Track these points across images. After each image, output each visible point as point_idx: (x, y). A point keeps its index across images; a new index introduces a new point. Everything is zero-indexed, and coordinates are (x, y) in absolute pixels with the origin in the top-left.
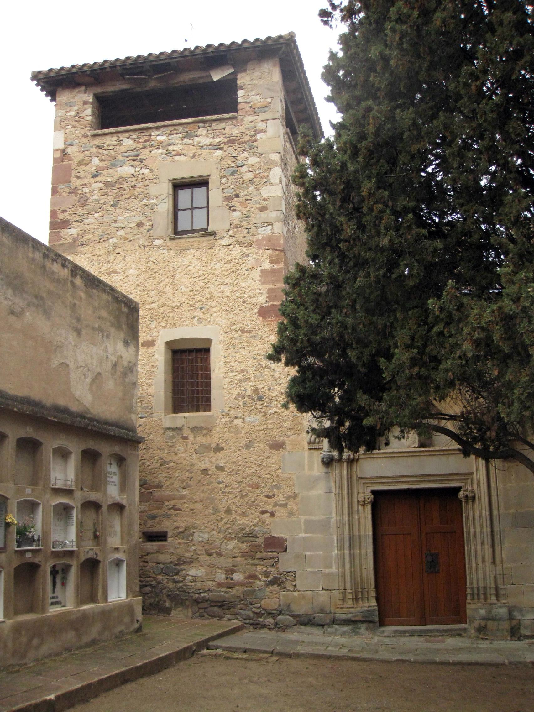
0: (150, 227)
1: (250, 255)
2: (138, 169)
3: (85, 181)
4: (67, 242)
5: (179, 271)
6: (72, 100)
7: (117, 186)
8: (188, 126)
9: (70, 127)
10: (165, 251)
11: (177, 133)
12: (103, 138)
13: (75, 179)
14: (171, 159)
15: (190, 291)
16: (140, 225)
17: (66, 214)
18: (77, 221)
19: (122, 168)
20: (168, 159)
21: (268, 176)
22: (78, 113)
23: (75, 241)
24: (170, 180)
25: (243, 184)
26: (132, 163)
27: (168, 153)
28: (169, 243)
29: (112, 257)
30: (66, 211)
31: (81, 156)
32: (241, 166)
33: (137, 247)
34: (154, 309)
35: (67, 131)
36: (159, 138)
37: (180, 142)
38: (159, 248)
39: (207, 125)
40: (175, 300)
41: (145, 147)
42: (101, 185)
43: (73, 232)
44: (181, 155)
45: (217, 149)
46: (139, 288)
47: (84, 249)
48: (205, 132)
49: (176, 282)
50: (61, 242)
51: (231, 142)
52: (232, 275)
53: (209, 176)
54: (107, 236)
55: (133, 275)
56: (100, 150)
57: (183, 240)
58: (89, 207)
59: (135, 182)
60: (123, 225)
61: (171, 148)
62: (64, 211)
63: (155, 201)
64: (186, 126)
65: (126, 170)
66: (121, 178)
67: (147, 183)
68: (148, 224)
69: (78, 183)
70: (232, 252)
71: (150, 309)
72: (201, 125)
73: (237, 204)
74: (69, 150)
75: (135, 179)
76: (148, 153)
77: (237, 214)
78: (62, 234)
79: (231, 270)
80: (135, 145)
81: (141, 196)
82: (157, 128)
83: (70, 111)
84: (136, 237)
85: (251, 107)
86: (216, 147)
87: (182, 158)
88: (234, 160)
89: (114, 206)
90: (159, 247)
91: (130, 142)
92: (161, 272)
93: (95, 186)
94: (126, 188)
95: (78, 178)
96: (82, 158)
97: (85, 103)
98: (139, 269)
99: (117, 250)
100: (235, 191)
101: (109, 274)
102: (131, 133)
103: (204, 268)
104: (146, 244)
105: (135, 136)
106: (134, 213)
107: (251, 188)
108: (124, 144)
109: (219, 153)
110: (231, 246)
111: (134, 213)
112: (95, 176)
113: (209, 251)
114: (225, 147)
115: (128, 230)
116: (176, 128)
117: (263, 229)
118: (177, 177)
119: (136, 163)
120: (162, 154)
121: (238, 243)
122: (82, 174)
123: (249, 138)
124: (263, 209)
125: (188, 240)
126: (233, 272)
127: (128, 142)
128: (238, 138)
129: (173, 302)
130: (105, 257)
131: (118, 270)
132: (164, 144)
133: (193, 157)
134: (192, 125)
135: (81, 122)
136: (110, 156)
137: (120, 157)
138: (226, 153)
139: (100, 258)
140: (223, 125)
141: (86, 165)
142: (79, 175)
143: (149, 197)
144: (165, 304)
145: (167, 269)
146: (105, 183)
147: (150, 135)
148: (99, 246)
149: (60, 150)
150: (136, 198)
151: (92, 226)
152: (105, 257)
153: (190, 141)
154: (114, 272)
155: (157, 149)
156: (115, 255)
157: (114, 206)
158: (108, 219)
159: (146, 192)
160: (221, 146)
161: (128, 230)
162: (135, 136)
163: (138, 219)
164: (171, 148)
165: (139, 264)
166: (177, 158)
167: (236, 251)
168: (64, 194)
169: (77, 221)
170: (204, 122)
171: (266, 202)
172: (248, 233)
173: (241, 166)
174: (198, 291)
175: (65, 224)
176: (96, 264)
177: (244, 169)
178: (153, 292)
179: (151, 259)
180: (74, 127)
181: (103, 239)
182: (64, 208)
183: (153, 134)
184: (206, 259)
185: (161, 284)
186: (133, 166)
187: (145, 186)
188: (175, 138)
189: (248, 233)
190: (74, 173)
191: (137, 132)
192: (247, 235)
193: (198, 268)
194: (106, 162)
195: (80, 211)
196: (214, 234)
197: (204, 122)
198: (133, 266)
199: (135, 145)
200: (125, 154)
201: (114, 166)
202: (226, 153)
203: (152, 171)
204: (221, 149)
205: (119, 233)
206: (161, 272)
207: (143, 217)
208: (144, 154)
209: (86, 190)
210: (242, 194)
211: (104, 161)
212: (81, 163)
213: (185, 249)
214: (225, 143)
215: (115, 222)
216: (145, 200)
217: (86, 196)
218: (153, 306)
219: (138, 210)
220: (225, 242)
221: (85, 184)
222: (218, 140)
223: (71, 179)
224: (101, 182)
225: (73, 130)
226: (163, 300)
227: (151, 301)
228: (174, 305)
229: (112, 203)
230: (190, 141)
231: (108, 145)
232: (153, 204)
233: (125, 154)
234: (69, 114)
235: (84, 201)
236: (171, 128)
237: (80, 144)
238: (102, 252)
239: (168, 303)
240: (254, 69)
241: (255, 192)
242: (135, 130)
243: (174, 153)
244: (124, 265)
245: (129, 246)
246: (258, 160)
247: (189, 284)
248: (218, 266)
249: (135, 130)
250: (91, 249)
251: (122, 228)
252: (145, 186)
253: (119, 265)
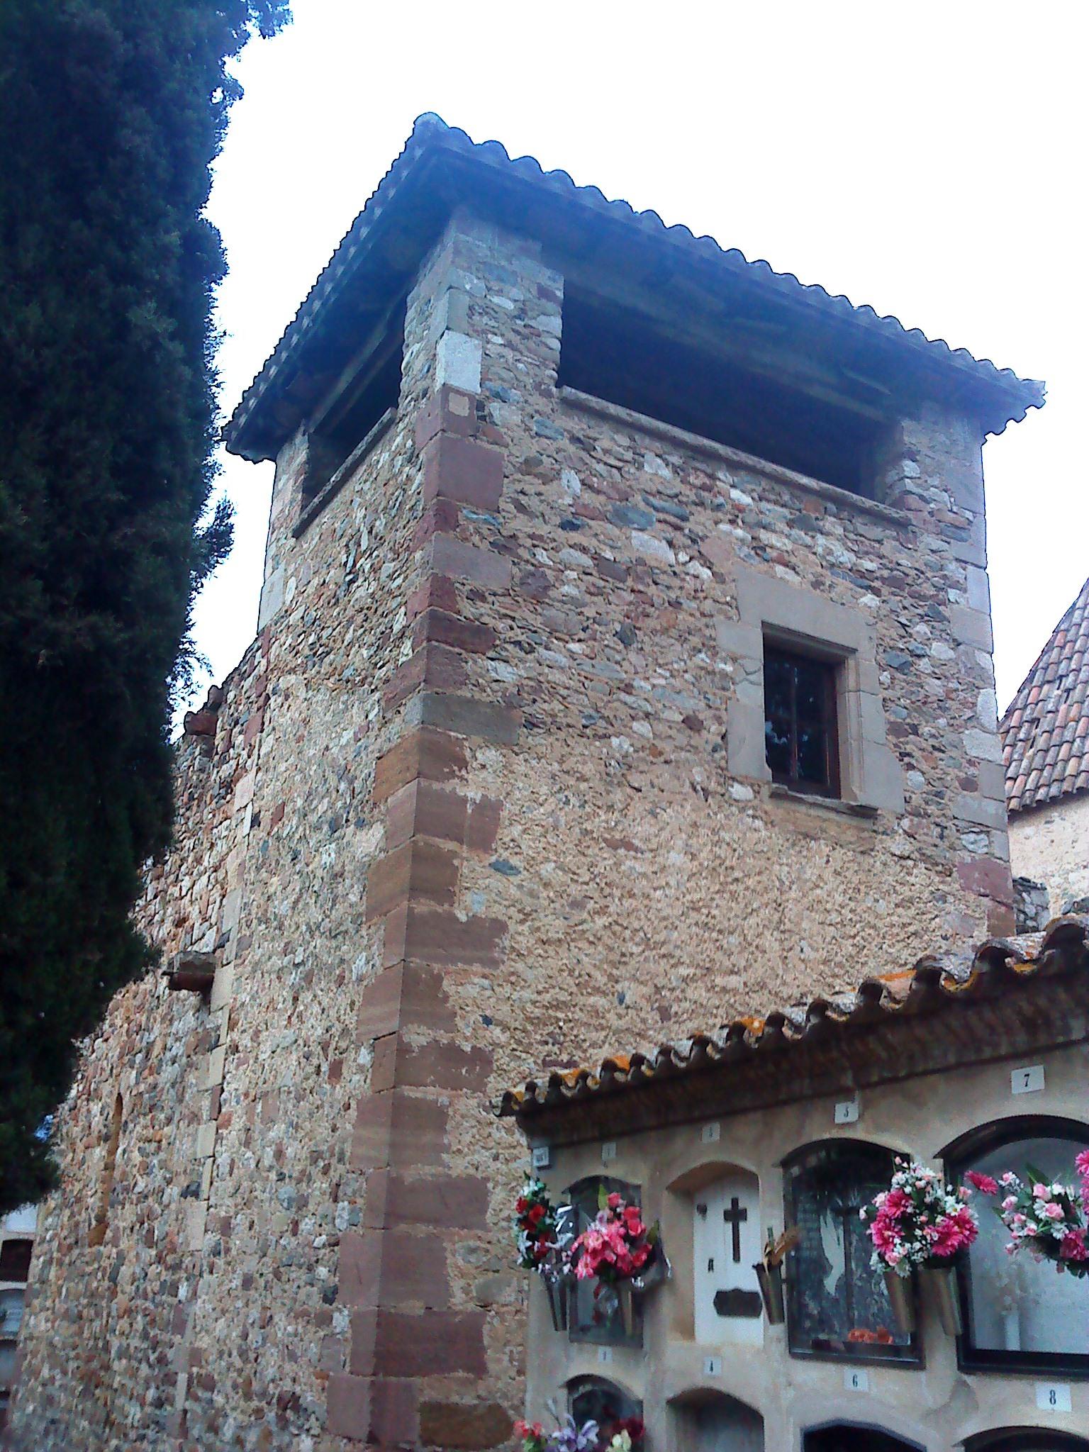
0: (720, 741)
1: (950, 899)
2: (683, 557)
3: (543, 530)
4: (484, 697)
5: (793, 894)
6: (503, 263)
7: (630, 582)
8: (806, 498)
9: (500, 340)
10: (758, 823)
11: (776, 503)
12: (592, 423)
13: (511, 507)
14: (764, 566)
15: (826, 962)
16: (692, 723)
17: (484, 608)
18: (518, 643)
19: (645, 536)
20: (758, 565)
21: (974, 704)
22: (523, 311)
23: (511, 703)
24: (764, 624)
25: (925, 703)
26: (671, 534)
27: (760, 549)
28: (769, 806)
29: (618, 796)
30: (483, 599)
31: (531, 448)
32: (919, 656)
33: (687, 788)
34: (735, 991)
35: (492, 349)
36: (735, 494)
37: (786, 530)
38: (742, 810)
39: (845, 515)
40: (788, 978)
41: (701, 504)
42: (586, 561)
43: (505, 672)
44: (786, 565)
45: (869, 588)
46: (693, 914)
47: (538, 740)
48: (840, 531)
49: (788, 926)
50: (465, 693)
51: (897, 583)
52: (915, 942)
53: (854, 651)
54: (602, 723)
55: (680, 871)
56: (584, 454)
57: (803, 809)
58: (553, 612)
59: (679, 593)
60: (650, 709)
61: (765, 536)
62: (476, 596)
63: (729, 668)
64: (798, 493)
65: (650, 545)
66: (641, 561)
67: (708, 606)
68: (713, 728)
69: (519, 524)
70: (912, 879)
71: (724, 990)
72: (832, 507)
73: (917, 754)
74: (495, 408)
75: (677, 582)
76: (709, 524)
77: (916, 777)
78: (469, 667)
79: (911, 929)
80: (678, 487)
81: (695, 640)
82: (734, 466)
83: (500, 293)
84: (683, 754)
85: (931, 513)
86: (864, 580)
87: (790, 576)
88: (902, 632)
89: (625, 638)
90: (743, 806)
91: (666, 473)
92: (750, 882)
93: (568, 554)
94: (657, 601)
95: (521, 508)
96: (533, 453)
97: (544, 293)
98: (694, 857)
99: (636, 779)
100: (909, 715)
101: (613, 845)
102: (668, 448)
103: (852, 904)
104: (713, 786)
105: (675, 459)
106: (677, 683)
107: (942, 722)
108: (646, 468)
109: (869, 599)
110: (910, 863)
111: (677, 683)
112: (568, 526)
113: (860, 858)
114: (885, 590)
115: (661, 728)
116: (777, 488)
117: (972, 837)
118: (782, 624)
119: (679, 539)
120: (742, 540)
121: (925, 858)
122: (532, 503)
123: (932, 592)
124: (969, 785)
125: (813, 812)
126: (915, 934)
127: (657, 470)
128: (909, 580)
129: (784, 983)
130: (601, 789)
131: (636, 842)
132: (751, 518)
133: (817, 584)
134: (814, 498)
135: (531, 344)
136: (613, 485)
137: (638, 498)
138: (887, 607)
139: (583, 786)
140: (877, 532)
141: (546, 480)
142: (524, 500)
143: (714, 652)
144: (763, 986)
145: (764, 878)
146: (597, 557)
147: (712, 477)
148: (579, 747)
149: (471, 397)
150: (682, 639)
151: (556, 676)
152: (601, 789)
153: (808, 540)
154: (629, 846)
155: (732, 522)
156: (629, 790)
157: (625, 638)
158: (604, 671)
159: (707, 632)
160: (877, 584)
161: (661, 728)
162: (675, 459)
163: (693, 704)
164: (765, 536)
165: (693, 841)
166: (780, 569)
167: (920, 875)
168: (476, 539)
169: (518, 643)
170: (841, 503)
171: (972, 771)
172: (942, 837)
173: (919, 656)
174: (840, 965)
175: (479, 638)
176: (573, 800)
177: (924, 664)
178: (732, 939)
179: (726, 836)
180: (509, 345)
181: (596, 727)
182: (477, 584)
183: (720, 475)
184: (855, 880)
185: (752, 921)
186: (670, 544)
187: (703, 615)
188: (775, 513)
189: (942, 837)
190: (509, 488)
191: (682, 452)
192: (938, 841)
193: (839, 899)
194: (602, 498)
195: (524, 613)
196: (865, 813)
197: (841, 503)
198: (680, 843)
199: (678, 487)
200: (656, 501)
201: (621, 518)
202: (887, 607)
203: (719, 577)
204: (876, 592)
205: (635, 725)
206: (750, 882)
207: (702, 704)
208: (700, 521)
209: (542, 556)
210: (925, 729)
211: (598, 492)
212: (529, 466)
213: (806, 836)
214: (883, 579)
215: (628, 688)
216: (702, 655)
217: (544, 575)
218: (734, 981)
219: (687, 676)
220: (899, 845)
221: (541, 538)
222: (868, 565)
223: (502, 505)
224: (584, 550)
225: (510, 354)
226: (757, 972)
227: (727, 963)
228: (785, 992)
229: (618, 627)
230: (808, 540)
231: (606, 451)
232: (724, 675)
233: (656, 501)
234: (496, 300)
235: (537, 589)
236: (765, 483)
237: (530, 410)
238: (589, 769)
239: (773, 984)
240: (935, 423)
241: (950, 736)
242: (677, 444)
243: (774, 554)
244: (654, 830)
245: (664, 775)
246: (951, 654)
247: (820, 939)
248: (882, 907)
249: (677, 444)
250: (559, 749)
251: (647, 715)
252: (703, 615)
253: (641, 830)
